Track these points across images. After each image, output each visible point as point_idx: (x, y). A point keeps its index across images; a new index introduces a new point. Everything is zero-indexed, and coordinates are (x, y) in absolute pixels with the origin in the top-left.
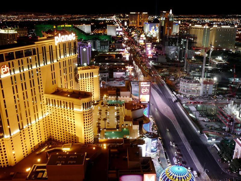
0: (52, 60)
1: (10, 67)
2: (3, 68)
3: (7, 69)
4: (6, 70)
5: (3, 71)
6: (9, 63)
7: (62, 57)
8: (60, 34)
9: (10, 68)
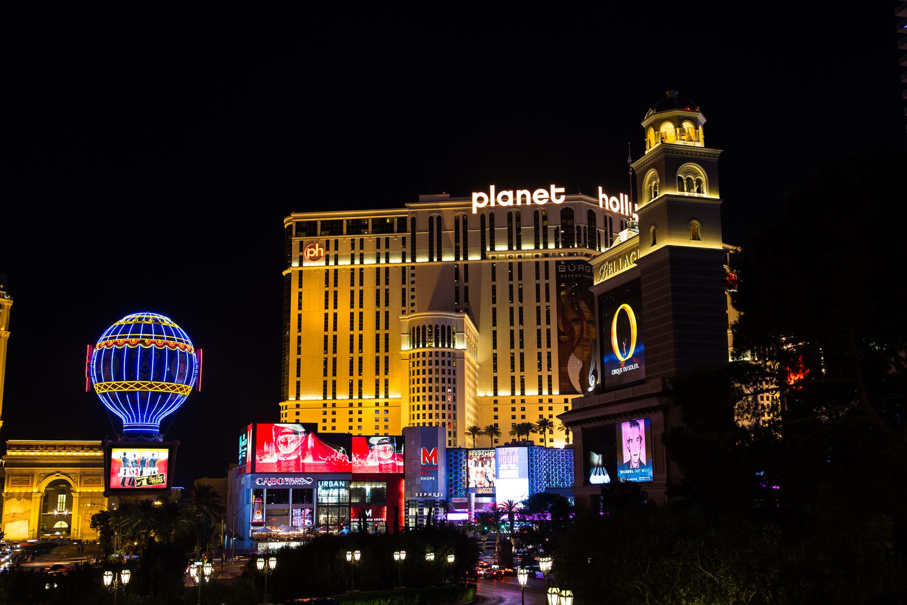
0: (462, 250)
1: (327, 249)
3: (319, 252)
4: (316, 252)
5: (309, 254)
6: (328, 242)
7: (502, 247)
8: (492, 188)
9: (327, 253)
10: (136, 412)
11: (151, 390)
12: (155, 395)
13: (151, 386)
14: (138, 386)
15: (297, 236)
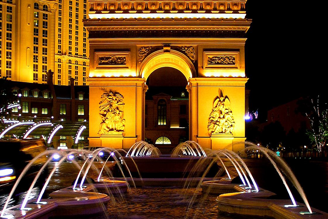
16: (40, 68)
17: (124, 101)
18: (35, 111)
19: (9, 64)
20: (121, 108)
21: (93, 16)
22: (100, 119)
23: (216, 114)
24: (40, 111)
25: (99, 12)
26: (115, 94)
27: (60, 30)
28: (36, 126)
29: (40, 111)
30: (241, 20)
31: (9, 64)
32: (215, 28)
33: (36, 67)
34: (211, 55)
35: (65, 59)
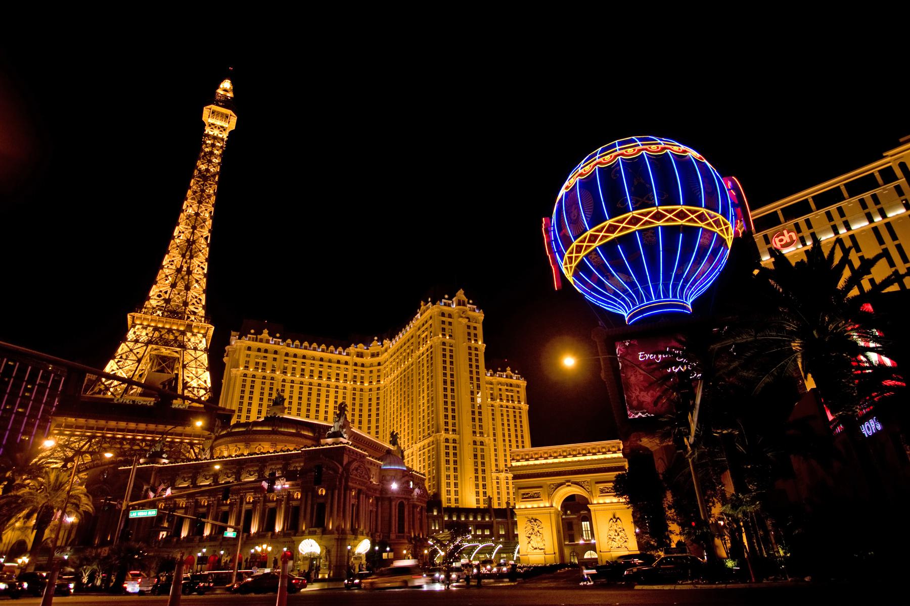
2: (777, 237)
3: (791, 237)
4: (786, 239)
6: (797, 226)
9: (801, 235)
10: (643, 281)
11: (661, 223)
12: (671, 232)
13: (658, 216)
14: (634, 221)
15: (758, 231)
16: (481, 494)
17: (542, 525)
18: (479, 533)
19: (456, 493)
20: (541, 531)
21: (514, 464)
22: (527, 540)
23: (613, 533)
24: (483, 532)
25: (518, 461)
26: (536, 520)
27: (496, 455)
28: (481, 546)
29: (483, 532)
30: (619, 458)
31: (456, 493)
32: (601, 466)
33: (477, 493)
34: (601, 486)
35: (503, 475)
